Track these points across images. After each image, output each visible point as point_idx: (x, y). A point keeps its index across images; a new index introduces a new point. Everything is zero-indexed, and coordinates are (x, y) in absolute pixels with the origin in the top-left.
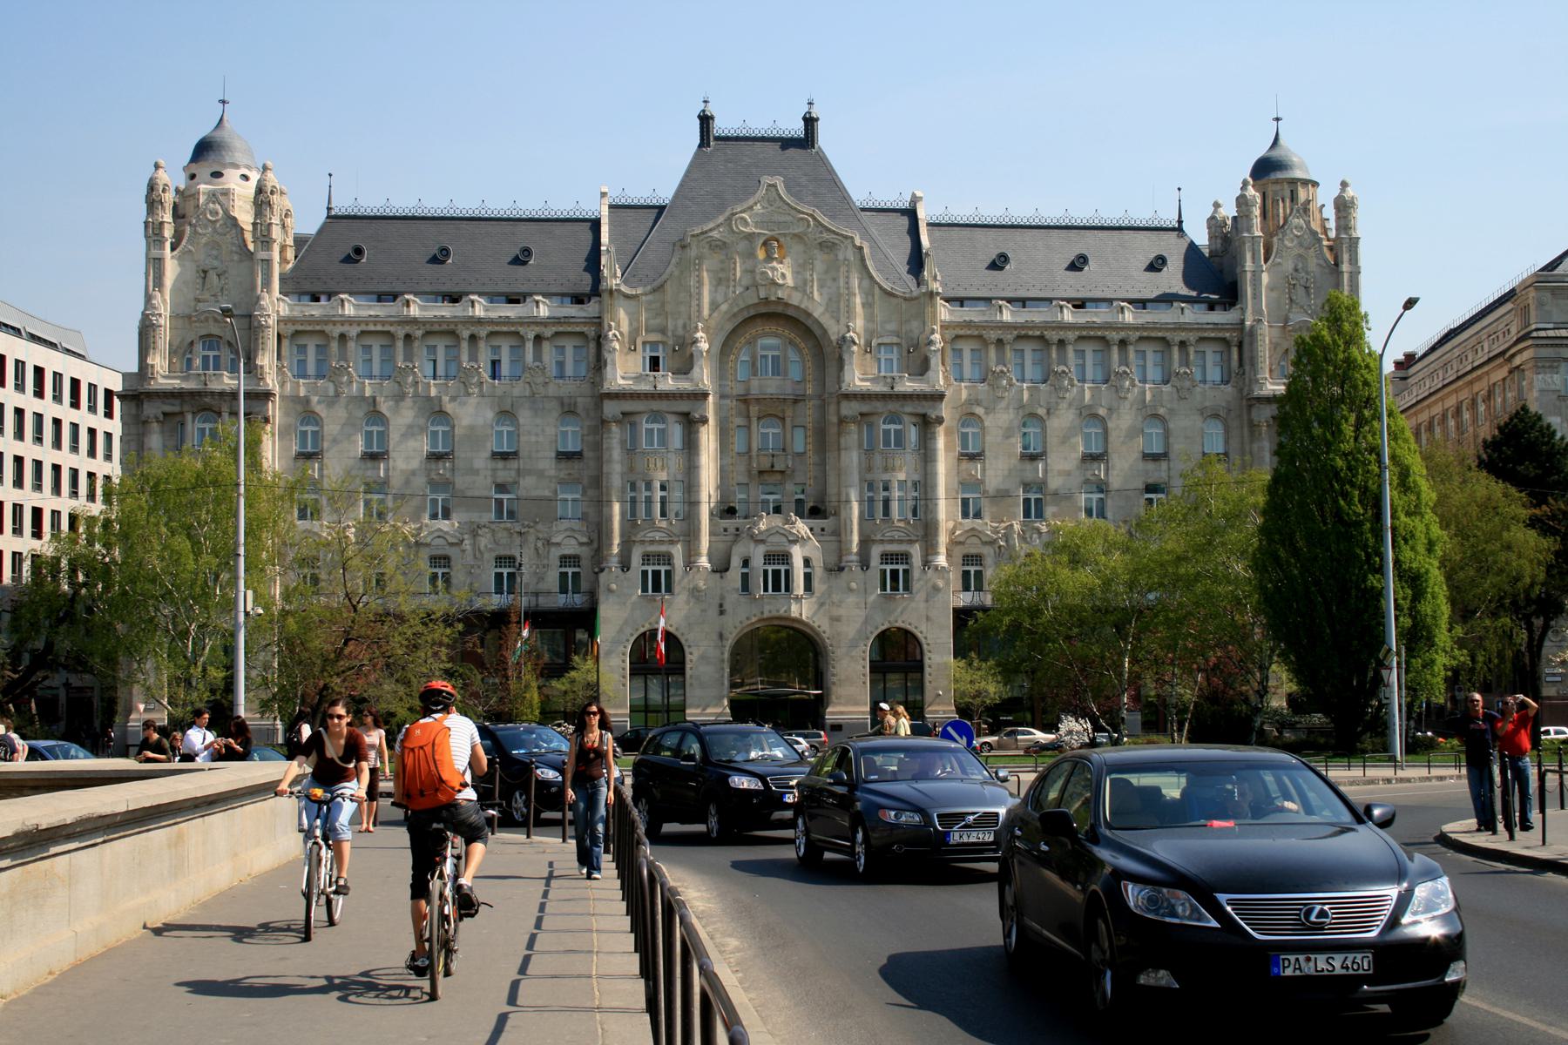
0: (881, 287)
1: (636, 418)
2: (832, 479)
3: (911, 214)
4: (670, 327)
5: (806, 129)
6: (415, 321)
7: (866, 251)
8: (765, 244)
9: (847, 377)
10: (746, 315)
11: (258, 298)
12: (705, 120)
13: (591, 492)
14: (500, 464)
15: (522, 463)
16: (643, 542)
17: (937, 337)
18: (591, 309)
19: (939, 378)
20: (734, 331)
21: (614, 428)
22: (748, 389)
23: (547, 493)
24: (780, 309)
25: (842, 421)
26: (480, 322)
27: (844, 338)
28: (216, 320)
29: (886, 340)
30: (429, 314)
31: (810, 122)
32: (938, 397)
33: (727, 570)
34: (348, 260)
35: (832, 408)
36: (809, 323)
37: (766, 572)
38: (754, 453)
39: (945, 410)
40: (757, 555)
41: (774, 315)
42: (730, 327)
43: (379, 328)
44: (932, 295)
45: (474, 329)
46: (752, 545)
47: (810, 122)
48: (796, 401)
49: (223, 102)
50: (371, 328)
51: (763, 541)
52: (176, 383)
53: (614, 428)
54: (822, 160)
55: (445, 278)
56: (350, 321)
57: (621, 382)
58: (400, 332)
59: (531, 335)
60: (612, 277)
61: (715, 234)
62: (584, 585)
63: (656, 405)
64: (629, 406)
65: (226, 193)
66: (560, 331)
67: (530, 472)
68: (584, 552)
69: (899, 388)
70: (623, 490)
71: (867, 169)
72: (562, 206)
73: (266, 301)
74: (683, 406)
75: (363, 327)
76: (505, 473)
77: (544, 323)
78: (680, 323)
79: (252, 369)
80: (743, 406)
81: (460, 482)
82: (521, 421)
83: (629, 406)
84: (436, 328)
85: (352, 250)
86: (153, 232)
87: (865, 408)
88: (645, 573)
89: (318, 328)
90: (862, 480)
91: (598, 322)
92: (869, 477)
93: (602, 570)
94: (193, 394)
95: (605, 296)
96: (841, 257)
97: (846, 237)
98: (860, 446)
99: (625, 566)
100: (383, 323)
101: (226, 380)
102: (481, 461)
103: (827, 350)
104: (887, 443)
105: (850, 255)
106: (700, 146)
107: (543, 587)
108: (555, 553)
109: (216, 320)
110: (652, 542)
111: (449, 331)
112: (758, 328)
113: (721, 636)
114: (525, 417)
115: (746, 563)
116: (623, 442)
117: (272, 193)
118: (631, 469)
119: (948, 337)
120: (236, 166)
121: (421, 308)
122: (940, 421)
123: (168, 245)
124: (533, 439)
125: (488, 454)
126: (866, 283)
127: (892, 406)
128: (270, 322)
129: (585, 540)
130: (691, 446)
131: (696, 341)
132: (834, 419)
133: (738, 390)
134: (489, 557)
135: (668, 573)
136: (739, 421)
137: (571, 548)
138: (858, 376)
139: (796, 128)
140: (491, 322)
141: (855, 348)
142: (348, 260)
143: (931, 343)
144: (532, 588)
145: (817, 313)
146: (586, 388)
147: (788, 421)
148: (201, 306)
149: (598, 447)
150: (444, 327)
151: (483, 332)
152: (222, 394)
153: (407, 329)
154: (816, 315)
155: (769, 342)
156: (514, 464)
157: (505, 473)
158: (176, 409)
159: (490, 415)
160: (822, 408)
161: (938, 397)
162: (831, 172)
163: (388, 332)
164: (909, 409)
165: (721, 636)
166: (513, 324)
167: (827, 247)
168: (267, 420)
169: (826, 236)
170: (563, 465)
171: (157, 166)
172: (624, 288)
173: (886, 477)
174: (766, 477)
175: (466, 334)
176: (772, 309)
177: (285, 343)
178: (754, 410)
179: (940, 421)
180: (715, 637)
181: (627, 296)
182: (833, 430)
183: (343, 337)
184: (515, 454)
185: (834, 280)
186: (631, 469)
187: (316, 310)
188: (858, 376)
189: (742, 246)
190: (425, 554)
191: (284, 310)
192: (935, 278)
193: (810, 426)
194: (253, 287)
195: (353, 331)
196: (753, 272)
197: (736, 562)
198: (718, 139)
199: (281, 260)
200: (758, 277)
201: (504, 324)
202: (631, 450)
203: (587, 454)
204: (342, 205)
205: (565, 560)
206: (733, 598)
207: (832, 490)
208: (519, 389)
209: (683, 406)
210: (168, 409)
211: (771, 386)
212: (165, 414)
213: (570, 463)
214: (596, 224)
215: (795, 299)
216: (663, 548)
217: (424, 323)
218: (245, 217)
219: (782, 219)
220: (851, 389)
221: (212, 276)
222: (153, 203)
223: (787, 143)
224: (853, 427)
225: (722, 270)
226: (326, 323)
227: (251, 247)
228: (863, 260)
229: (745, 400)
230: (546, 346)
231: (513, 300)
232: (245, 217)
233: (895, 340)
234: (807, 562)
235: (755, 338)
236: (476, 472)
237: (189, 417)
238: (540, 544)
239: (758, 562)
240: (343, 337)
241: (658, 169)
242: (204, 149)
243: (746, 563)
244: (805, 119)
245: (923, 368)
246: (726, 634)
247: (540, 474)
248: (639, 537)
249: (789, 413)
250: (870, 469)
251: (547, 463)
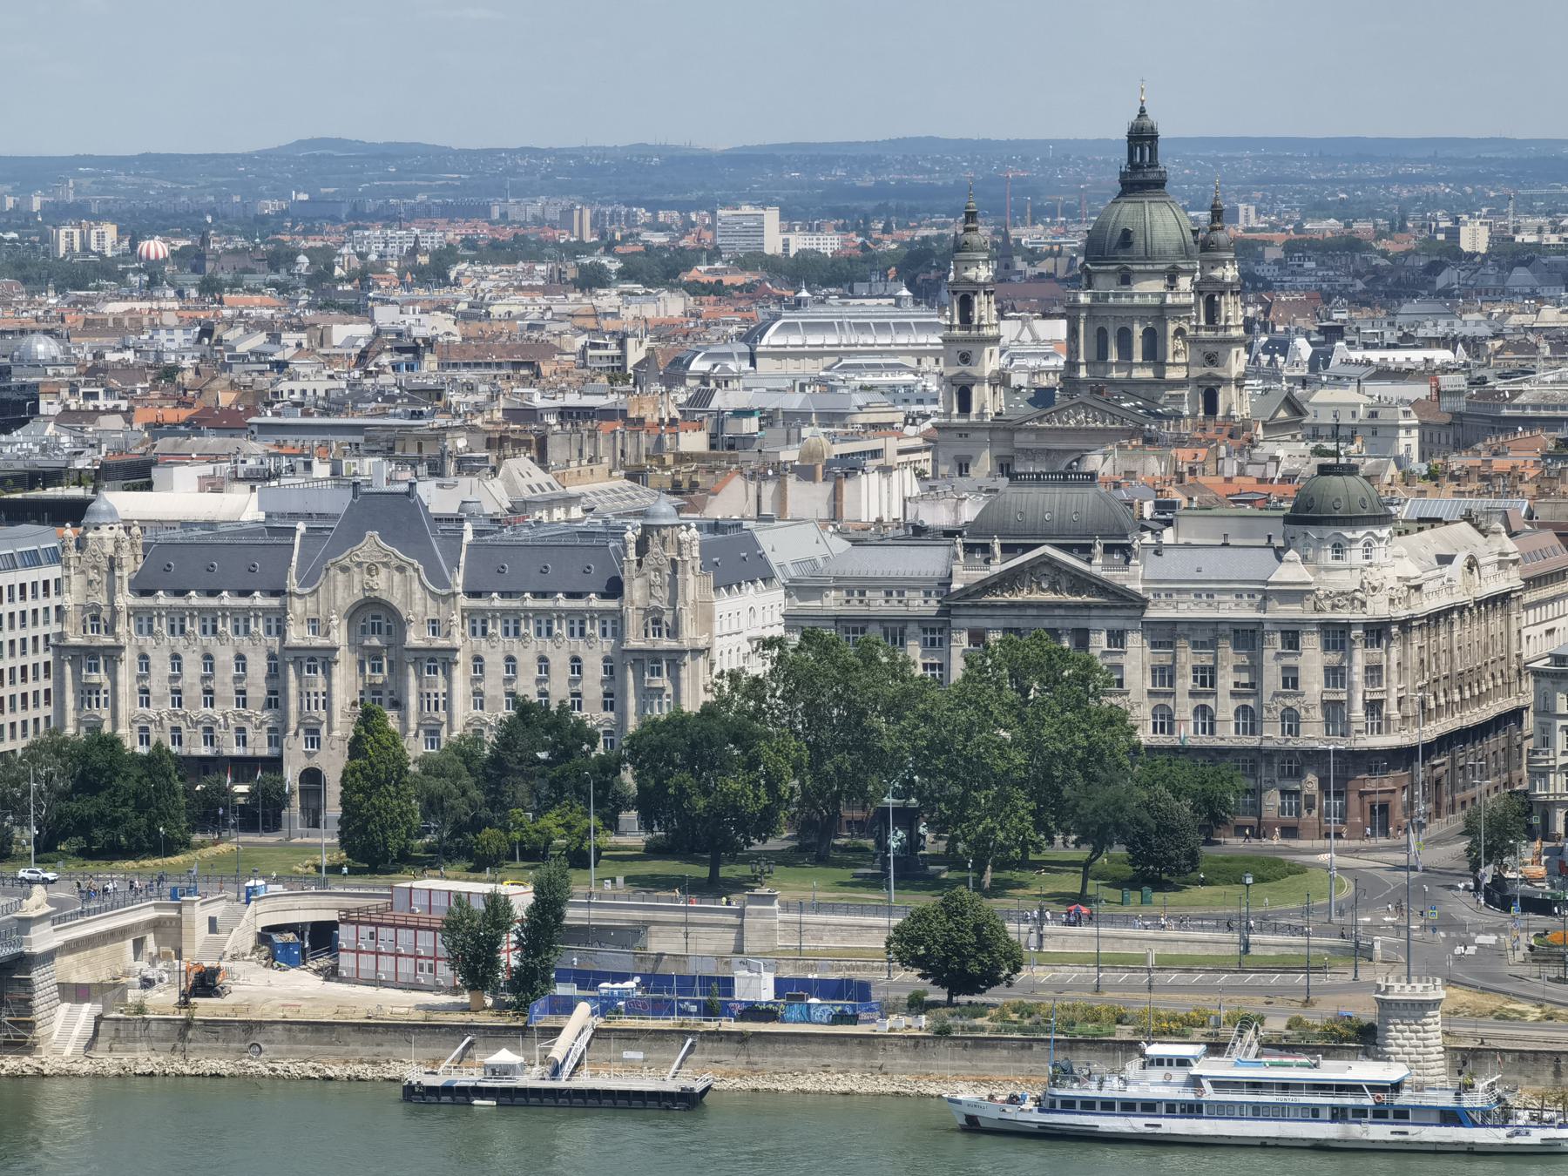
19: (457, 641)
32: (456, 650)
39: (459, 656)
64: (298, 654)
69: (435, 645)
76: (240, 686)
81: (217, 689)
83: (298, 654)
87: (418, 655)
102: (229, 680)
127: (431, 654)
134: (232, 730)
159: (232, 655)
179: (456, 663)
187: (147, 601)
190: (200, 727)
209: (324, 654)
236: (224, 684)
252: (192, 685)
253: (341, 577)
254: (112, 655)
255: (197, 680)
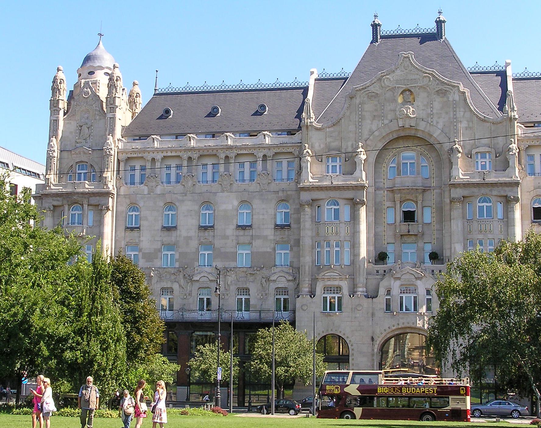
0: (477, 117)
1: (321, 203)
2: (447, 239)
3: (503, 74)
4: (344, 146)
5: (437, 28)
6: (193, 149)
7: (468, 94)
8: (402, 93)
9: (454, 173)
10: (391, 137)
11: (106, 139)
12: (375, 27)
13: (295, 249)
14: (241, 232)
15: (254, 232)
16: (323, 279)
17: (514, 146)
18: (296, 138)
19: (517, 174)
20: (385, 148)
21: (308, 209)
22: (394, 184)
23: (269, 250)
24: (413, 133)
25: (452, 201)
26: (231, 148)
27: (452, 149)
28: (84, 153)
29: (482, 149)
30: (201, 145)
31: (439, 23)
33: (377, 297)
34: (161, 118)
35: (447, 194)
36: (432, 141)
37: (401, 298)
38: (397, 224)
40: (396, 287)
41: (407, 137)
42: (380, 146)
43: (174, 154)
44: (511, 120)
45: (228, 153)
46: (392, 281)
47: (439, 23)
48: (424, 191)
49: (100, 35)
50: (169, 154)
51: (399, 278)
52: (60, 189)
53: (308, 209)
54: (447, 44)
55: (213, 124)
56: (158, 150)
57: (311, 180)
58: (185, 156)
59: (261, 155)
60: (311, 118)
61: (372, 89)
62: (290, 307)
63: (332, 194)
64: (316, 195)
65: (95, 83)
66: (278, 153)
67: (259, 237)
68: (291, 286)
69: (489, 180)
70: (313, 248)
71: (473, 49)
72: (286, 80)
73: (110, 139)
74: (349, 194)
75: (165, 154)
77: (269, 147)
78: (350, 144)
79: (101, 180)
80: (391, 195)
81: (218, 243)
82: (254, 206)
83: (316, 195)
84: (206, 153)
85: (164, 112)
86: (54, 105)
87: (466, 192)
88: (325, 299)
89: (140, 155)
90: (465, 239)
91: (300, 146)
92: (469, 237)
93: (298, 297)
94: (68, 194)
95: (304, 129)
96: (451, 99)
97: (454, 86)
98: (464, 217)
99: (312, 294)
100: (176, 151)
101: (87, 186)
102: (230, 230)
103: (445, 157)
104: (481, 214)
105: (457, 97)
106: (372, 43)
107: (265, 307)
108: (273, 286)
109: (84, 153)
110: (329, 279)
111: (212, 154)
112: (401, 144)
113: (373, 339)
114: (257, 204)
115: (389, 292)
116: (313, 218)
117: (117, 80)
118: (318, 234)
119: (522, 147)
120: (101, 68)
121: (198, 141)
122: (517, 200)
123: (61, 113)
124: (261, 217)
125: (234, 227)
126: (468, 114)
127: (484, 190)
128: (112, 152)
129: (291, 278)
130: (355, 218)
131: (357, 154)
132: (448, 201)
133: (388, 184)
134: (233, 288)
135: (340, 299)
136: (388, 204)
137: (282, 283)
138: (461, 173)
139: (430, 27)
140: (236, 147)
141: (460, 155)
142: (161, 118)
143: (510, 150)
144: (258, 308)
145: (436, 134)
146: (293, 185)
147: (419, 203)
148: (78, 145)
149: (298, 221)
150: (210, 152)
151: (232, 154)
152: (83, 194)
153: (189, 154)
154: (435, 135)
155: (409, 154)
156: (249, 232)
157: (244, 236)
158: (60, 203)
159: (236, 203)
160: (441, 195)
161: (517, 184)
162: (452, 52)
163: (178, 157)
164: (495, 193)
165: (373, 339)
166: (250, 148)
167: (442, 93)
168: (108, 209)
169: (441, 87)
170: (278, 232)
171: (58, 70)
172: (315, 124)
173: (480, 237)
174: (405, 238)
175: (223, 156)
176: (407, 133)
177: (122, 164)
178: (397, 196)
180: (369, 340)
181: (317, 129)
182: (447, 208)
183: (153, 159)
184: (250, 226)
185: (447, 113)
186: (318, 234)
187: (138, 145)
188: (461, 173)
189: (389, 95)
191: (121, 145)
192: (513, 109)
193: (434, 206)
194: (105, 135)
195: (159, 156)
196: (395, 111)
197: (382, 291)
198: (382, 37)
199: (123, 117)
200: (398, 113)
201: (245, 149)
202: (317, 222)
203: (292, 226)
204: (163, 87)
205: (278, 290)
206: (380, 314)
207: (446, 246)
208: (254, 187)
209: (349, 194)
210: (56, 203)
211: (407, 180)
212: (54, 206)
213: (282, 231)
214: (306, 90)
215: (422, 126)
216: (336, 283)
217: (199, 150)
218: (103, 93)
219: (413, 77)
220: (457, 181)
221: (85, 128)
222: (55, 89)
223: (425, 38)
224: (458, 205)
225: (376, 110)
226: (144, 152)
227: (105, 110)
228: (465, 100)
229: (392, 190)
230: (269, 163)
231: (251, 134)
232: (103, 93)
233: (487, 149)
234: (428, 292)
235: (399, 153)
236: (226, 237)
237: (66, 207)
238: (264, 280)
239: (396, 291)
240: (153, 159)
241: (346, 55)
242: (88, 59)
243: (389, 292)
244: (436, 21)
245: (506, 165)
246: (375, 338)
247: (265, 238)
248: (320, 276)
249: (420, 197)
250: (470, 232)
251: (269, 232)
252: (188, 239)
253: (369, 107)
254: (97, 202)
255: (193, 232)
